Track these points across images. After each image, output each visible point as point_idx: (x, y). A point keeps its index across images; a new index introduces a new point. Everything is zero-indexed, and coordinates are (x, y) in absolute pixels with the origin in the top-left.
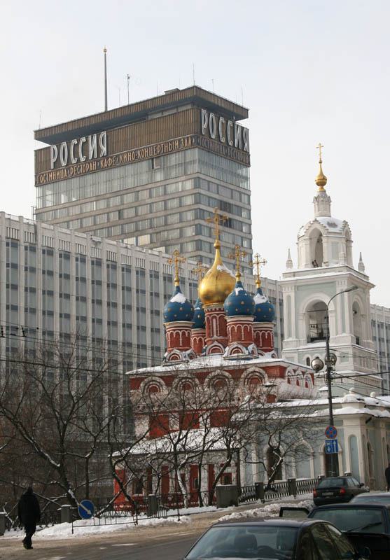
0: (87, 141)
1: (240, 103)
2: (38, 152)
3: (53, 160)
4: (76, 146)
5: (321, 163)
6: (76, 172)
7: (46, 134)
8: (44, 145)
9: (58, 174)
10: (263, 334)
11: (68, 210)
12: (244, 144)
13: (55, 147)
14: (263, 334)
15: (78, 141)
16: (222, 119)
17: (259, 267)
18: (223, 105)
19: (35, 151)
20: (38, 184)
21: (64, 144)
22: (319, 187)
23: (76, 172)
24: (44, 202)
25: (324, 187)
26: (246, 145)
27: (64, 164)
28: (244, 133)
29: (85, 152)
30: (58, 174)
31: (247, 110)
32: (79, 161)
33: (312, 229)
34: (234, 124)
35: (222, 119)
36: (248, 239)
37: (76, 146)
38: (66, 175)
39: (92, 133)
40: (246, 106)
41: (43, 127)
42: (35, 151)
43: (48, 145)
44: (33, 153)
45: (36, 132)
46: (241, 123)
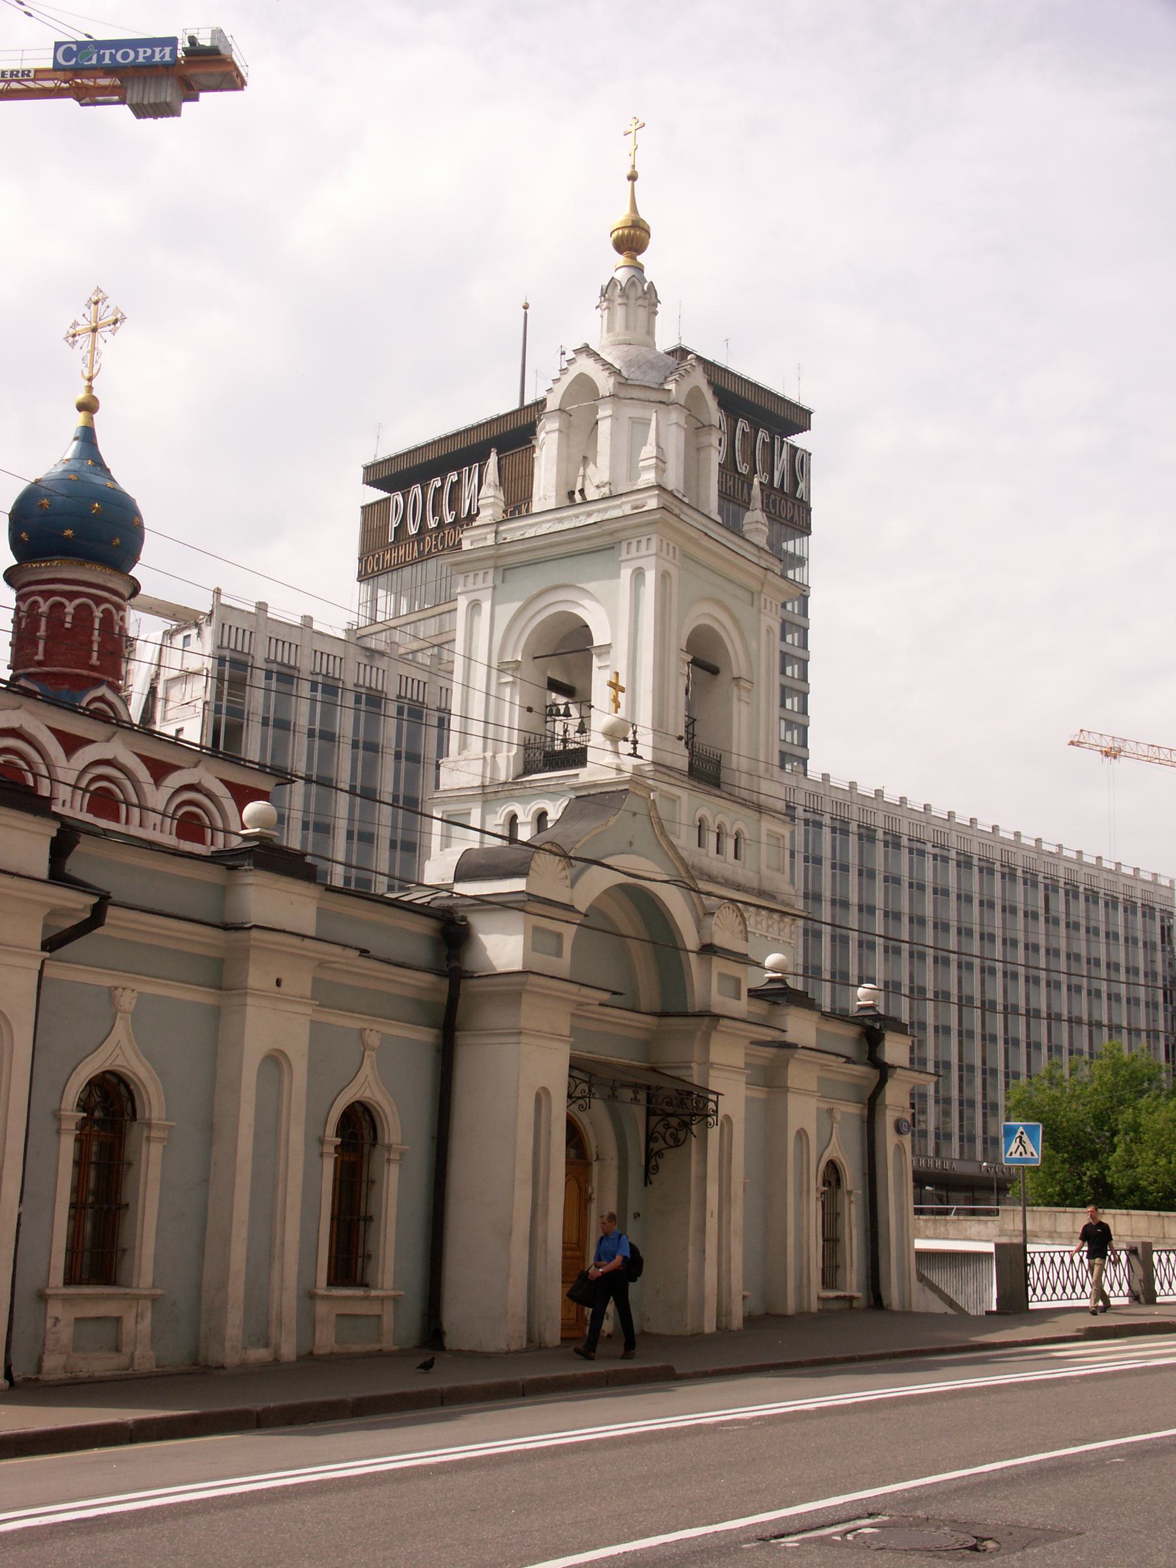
0: (459, 481)
1: (791, 395)
2: (367, 510)
3: (394, 524)
4: (439, 491)
5: (633, 178)
6: (436, 545)
7: (386, 472)
8: (379, 495)
9: (402, 552)
11: (416, 628)
12: (796, 484)
13: (400, 499)
15: (443, 481)
16: (742, 424)
17: (100, 344)
18: (749, 395)
19: (362, 507)
20: (364, 576)
21: (417, 490)
22: (621, 259)
23: (436, 545)
24: (374, 609)
25: (640, 258)
26: (802, 486)
27: (413, 530)
28: (799, 464)
29: (454, 503)
30: (402, 552)
31: (808, 413)
32: (441, 522)
33: (567, 379)
34: (772, 439)
35: (742, 424)
36: (801, 692)
37: (439, 491)
38: (416, 554)
39: (470, 464)
40: (805, 403)
41: (381, 456)
42: (362, 507)
43: (385, 495)
44: (360, 510)
45: (367, 469)
46: (798, 440)
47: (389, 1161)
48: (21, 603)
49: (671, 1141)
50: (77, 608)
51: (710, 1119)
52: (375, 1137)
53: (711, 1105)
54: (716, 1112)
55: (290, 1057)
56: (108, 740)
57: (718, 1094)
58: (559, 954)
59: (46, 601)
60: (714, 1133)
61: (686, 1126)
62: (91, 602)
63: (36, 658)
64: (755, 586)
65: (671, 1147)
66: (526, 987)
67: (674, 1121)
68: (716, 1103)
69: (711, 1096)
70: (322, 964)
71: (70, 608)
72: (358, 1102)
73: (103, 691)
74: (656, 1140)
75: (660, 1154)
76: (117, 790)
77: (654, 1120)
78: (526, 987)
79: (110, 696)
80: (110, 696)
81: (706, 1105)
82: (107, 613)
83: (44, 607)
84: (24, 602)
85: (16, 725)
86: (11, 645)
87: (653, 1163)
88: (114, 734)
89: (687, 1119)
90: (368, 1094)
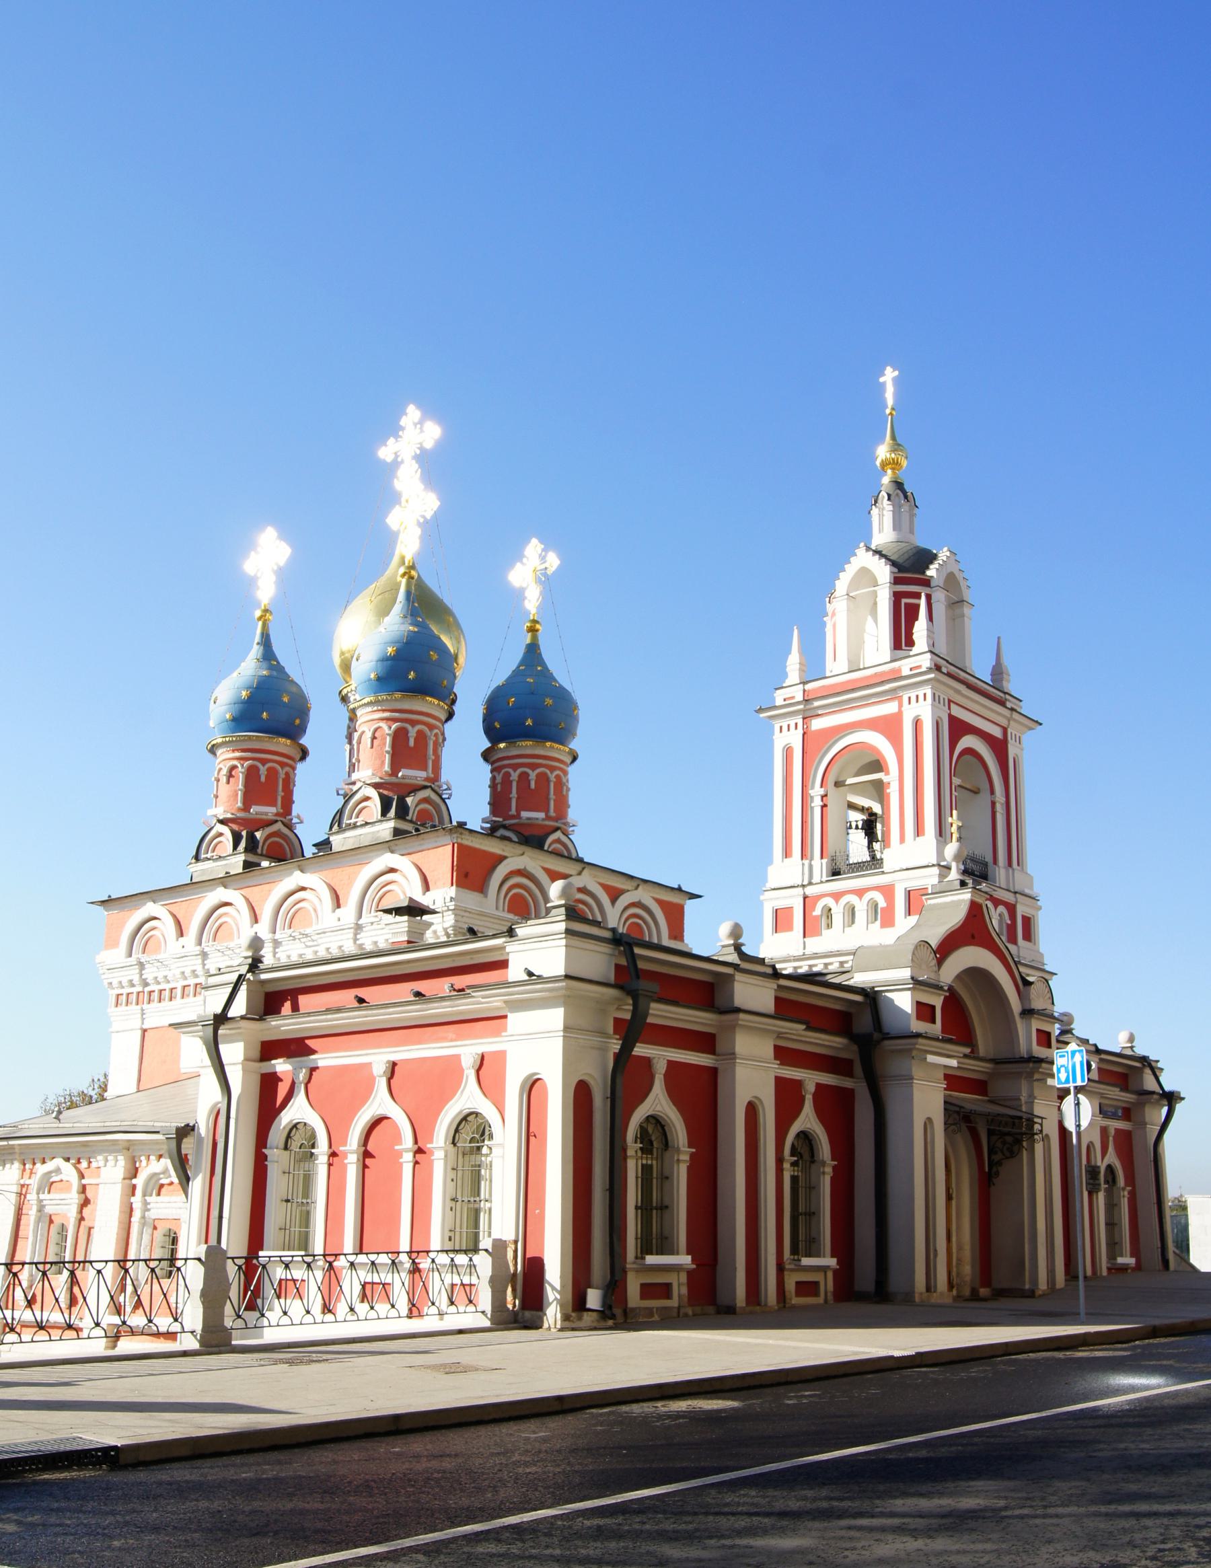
10: (524, 777)
14: (524, 777)
47: (824, 1173)
48: (496, 774)
49: (1008, 1154)
50: (537, 776)
51: (1036, 1137)
52: (812, 1155)
53: (1037, 1127)
54: (1041, 1131)
55: (764, 1102)
56: (580, 874)
57: (1042, 1118)
58: (933, 1021)
59: (515, 771)
60: (1039, 1148)
61: (1018, 1142)
62: (548, 772)
63: (510, 813)
64: (1004, 722)
65: (1007, 1158)
66: (917, 1046)
67: (1009, 1139)
68: (1041, 1125)
69: (1036, 1120)
70: (779, 1036)
71: (533, 775)
72: (801, 1132)
73: (558, 835)
74: (996, 1153)
75: (999, 1163)
76: (588, 911)
77: (994, 1138)
78: (917, 1046)
79: (564, 838)
80: (564, 838)
81: (1033, 1127)
82: (558, 777)
83: (515, 776)
84: (499, 773)
85: (521, 867)
86: (489, 804)
87: (994, 1169)
88: (583, 869)
89: (1019, 1137)
90: (809, 1126)
